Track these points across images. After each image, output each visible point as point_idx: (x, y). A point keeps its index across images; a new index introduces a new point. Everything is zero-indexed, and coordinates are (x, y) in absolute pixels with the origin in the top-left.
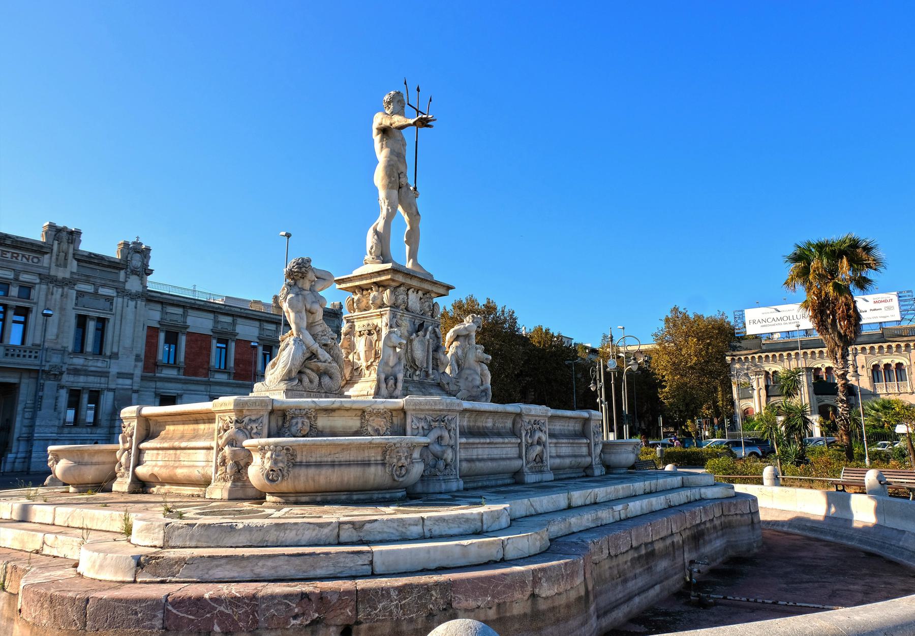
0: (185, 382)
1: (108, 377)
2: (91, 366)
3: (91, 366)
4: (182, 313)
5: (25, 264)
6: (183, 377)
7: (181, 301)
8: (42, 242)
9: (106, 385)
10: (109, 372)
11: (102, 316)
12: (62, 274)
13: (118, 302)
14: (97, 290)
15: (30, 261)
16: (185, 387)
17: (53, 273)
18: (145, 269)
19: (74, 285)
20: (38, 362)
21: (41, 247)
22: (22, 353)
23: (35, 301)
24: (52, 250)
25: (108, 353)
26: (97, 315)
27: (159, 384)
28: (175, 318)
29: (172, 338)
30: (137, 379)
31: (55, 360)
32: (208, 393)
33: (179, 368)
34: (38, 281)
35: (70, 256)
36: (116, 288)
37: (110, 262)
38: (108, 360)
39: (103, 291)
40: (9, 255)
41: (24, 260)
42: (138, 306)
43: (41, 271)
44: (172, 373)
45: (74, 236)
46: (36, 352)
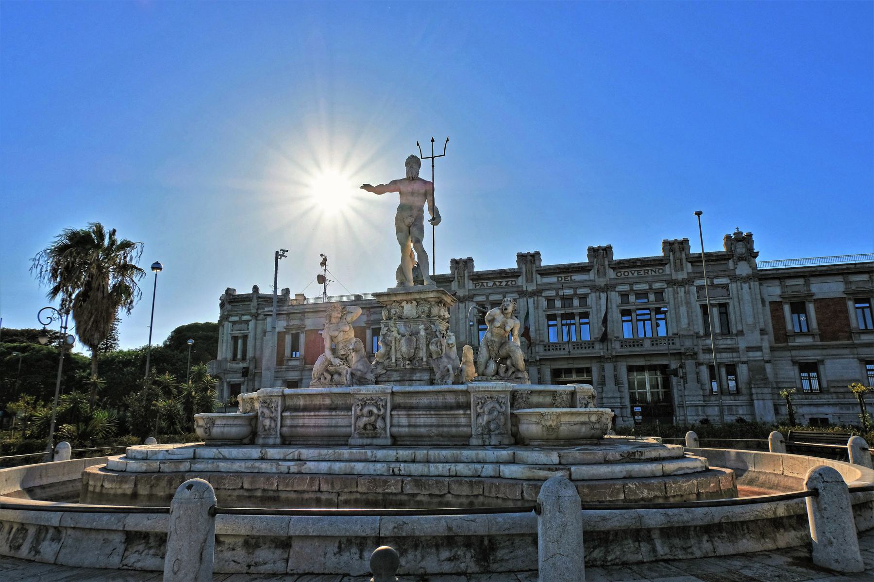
0: (824, 348)
1: (739, 352)
2: (722, 344)
3: (722, 344)
4: (803, 283)
5: (654, 276)
6: (820, 343)
7: (797, 272)
8: (662, 256)
9: (739, 359)
10: (738, 348)
11: (722, 302)
12: (681, 276)
13: (733, 287)
14: (713, 282)
15: (657, 273)
16: (824, 352)
17: (674, 277)
18: (750, 253)
19: (693, 282)
20: (666, 347)
21: (662, 260)
22: (663, 342)
23: (667, 301)
24: (670, 260)
25: (735, 332)
26: (717, 302)
27: (794, 353)
28: (797, 289)
29: (798, 308)
30: (766, 350)
31: (688, 343)
32: (856, 356)
33: (813, 335)
34: (666, 286)
35: (684, 261)
36: (728, 276)
37: (718, 256)
38: (736, 337)
39: (717, 281)
40: (642, 273)
41: (653, 273)
42: (752, 286)
43: (666, 278)
44: (808, 340)
45: (684, 244)
46: (673, 340)
